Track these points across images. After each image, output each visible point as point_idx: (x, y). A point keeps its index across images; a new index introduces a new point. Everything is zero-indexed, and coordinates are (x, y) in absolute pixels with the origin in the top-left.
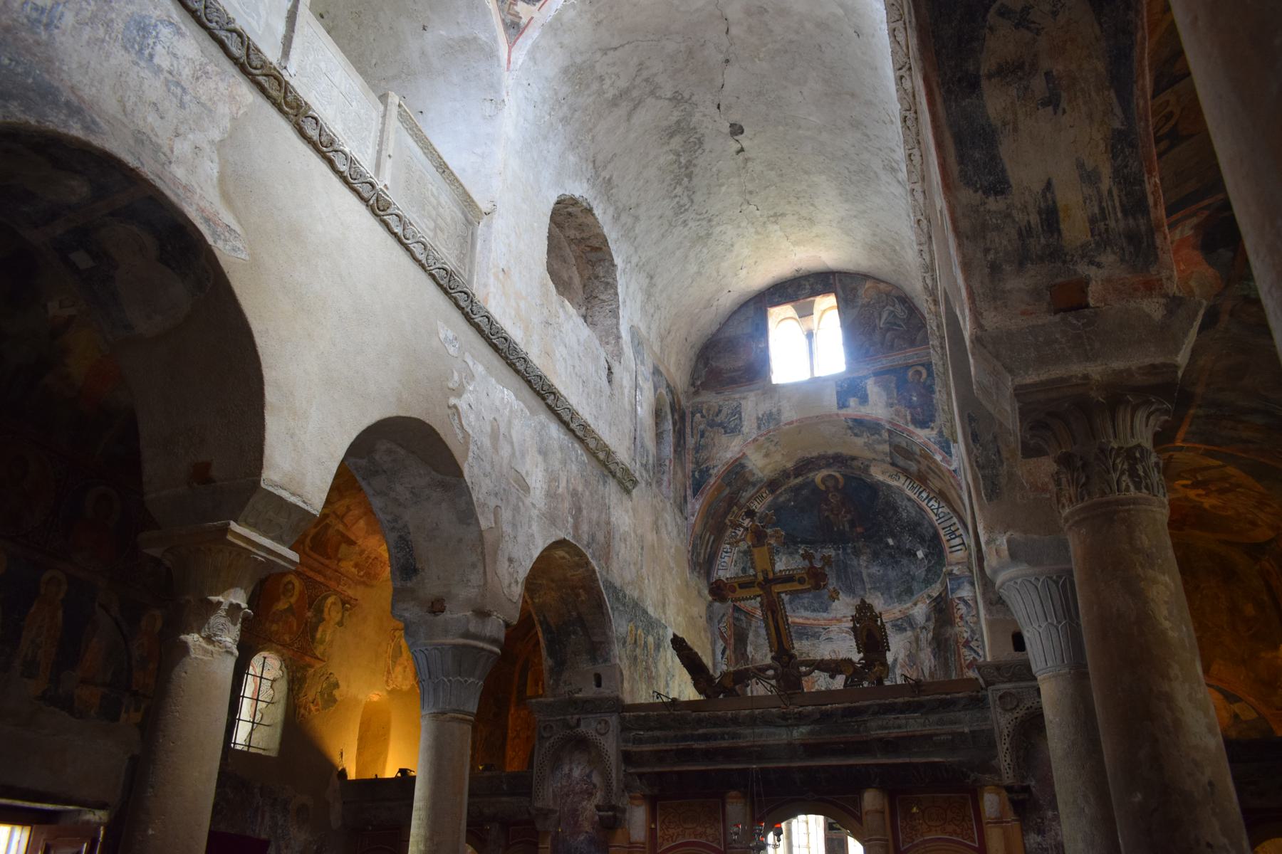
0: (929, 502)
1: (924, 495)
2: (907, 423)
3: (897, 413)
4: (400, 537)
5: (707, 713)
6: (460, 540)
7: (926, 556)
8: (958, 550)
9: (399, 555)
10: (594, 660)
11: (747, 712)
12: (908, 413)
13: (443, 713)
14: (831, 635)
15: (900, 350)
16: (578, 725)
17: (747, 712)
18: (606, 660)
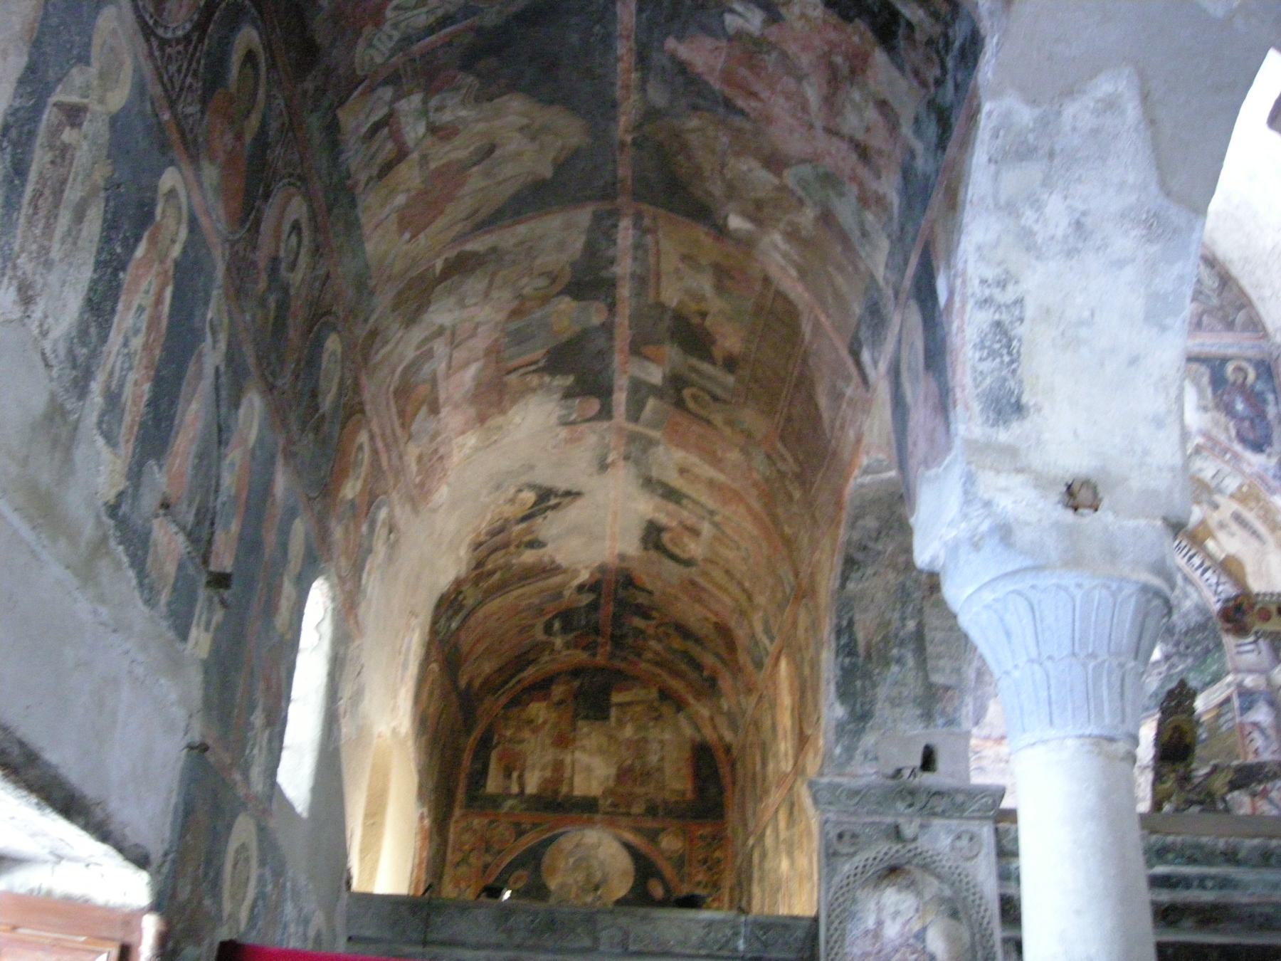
0: (1203, 574)
1: (1197, 561)
2: (1230, 439)
3: (1217, 423)
4: (998, 324)
5: (1179, 839)
6: (1134, 361)
7: (1167, 657)
8: (1248, 652)
9: (985, 366)
10: (928, 716)
11: (1256, 841)
12: (1231, 424)
13: (1111, 740)
14: (984, 763)
15: (1212, 330)
16: (915, 839)
17: (1256, 841)
18: (951, 722)
